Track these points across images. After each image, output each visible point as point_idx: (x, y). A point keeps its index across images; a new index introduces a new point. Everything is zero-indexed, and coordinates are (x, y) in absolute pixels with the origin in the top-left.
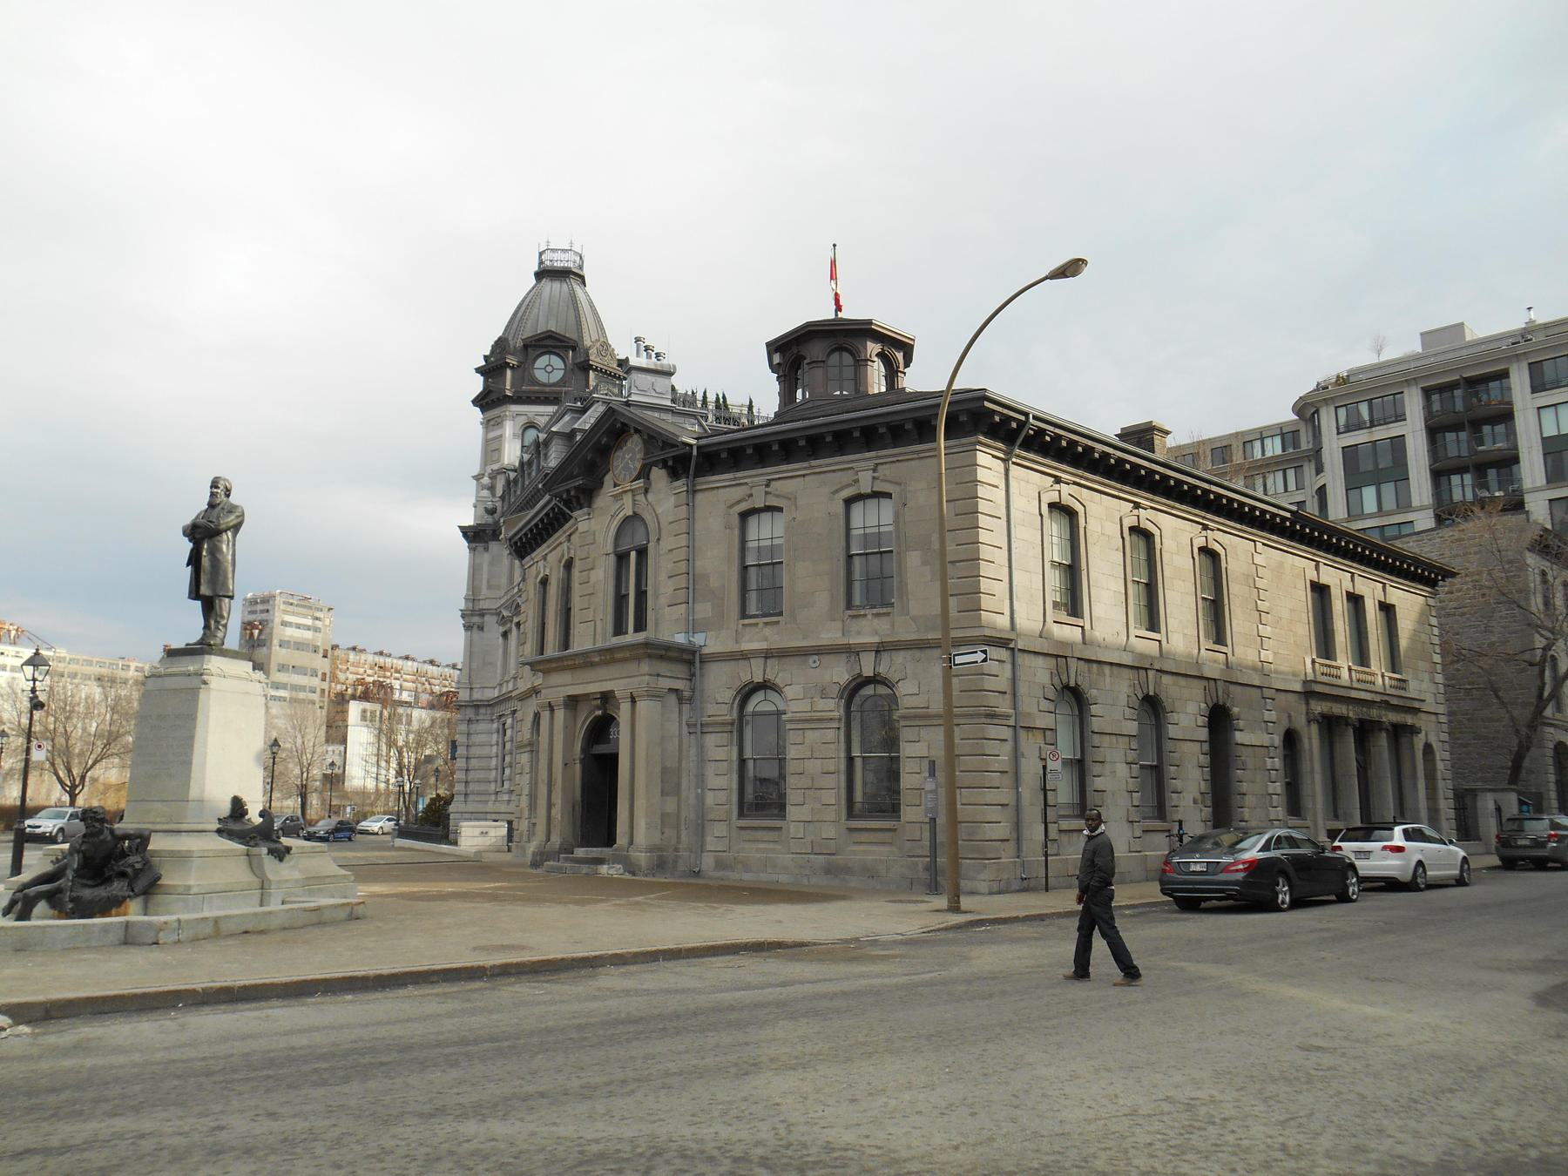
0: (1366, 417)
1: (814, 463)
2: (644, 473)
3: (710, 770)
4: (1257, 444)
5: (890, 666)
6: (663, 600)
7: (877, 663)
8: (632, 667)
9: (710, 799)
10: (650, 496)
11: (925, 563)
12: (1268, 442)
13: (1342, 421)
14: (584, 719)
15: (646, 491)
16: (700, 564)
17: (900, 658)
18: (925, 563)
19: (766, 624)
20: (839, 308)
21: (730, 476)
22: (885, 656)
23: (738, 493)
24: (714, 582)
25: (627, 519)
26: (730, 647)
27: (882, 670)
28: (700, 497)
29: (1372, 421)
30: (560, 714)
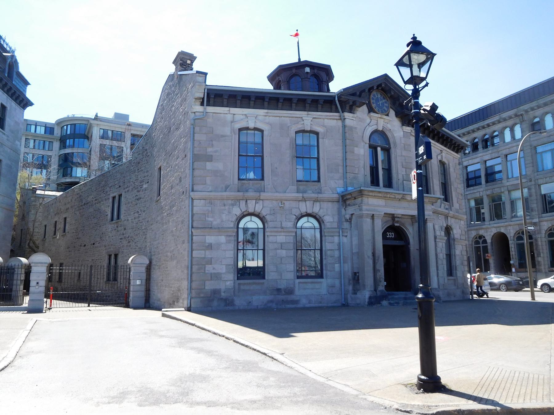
4: (33, 128)
12: (38, 128)
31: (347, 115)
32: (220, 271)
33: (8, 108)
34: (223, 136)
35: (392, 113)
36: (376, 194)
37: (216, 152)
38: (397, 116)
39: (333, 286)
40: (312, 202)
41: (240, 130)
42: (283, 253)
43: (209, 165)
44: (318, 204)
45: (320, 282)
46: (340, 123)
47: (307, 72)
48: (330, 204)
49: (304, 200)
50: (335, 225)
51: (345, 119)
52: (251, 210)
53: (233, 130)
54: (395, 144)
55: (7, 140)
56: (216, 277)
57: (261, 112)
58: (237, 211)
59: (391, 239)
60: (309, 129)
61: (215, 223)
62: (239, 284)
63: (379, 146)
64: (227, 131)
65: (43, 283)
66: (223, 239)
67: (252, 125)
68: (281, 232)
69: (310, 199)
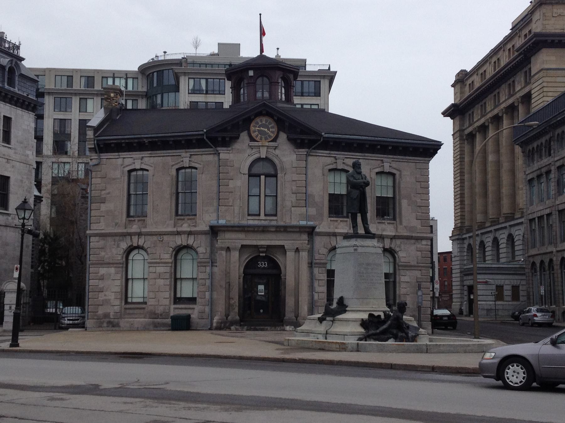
0: (204, 88)
1: (367, 155)
2: (274, 140)
3: (316, 284)
5: (395, 245)
6: (288, 204)
7: (391, 244)
8: (295, 236)
9: (316, 297)
10: (277, 151)
11: (409, 205)
13: (191, 87)
14: (246, 257)
15: (275, 149)
16: (310, 189)
17: (398, 242)
18: (409, 205)
19: (341, 221)
20: (262, 50)
21: (328, 152)
22: (394, 240)
23: (329, 160)
24: (317, 199)
25: (259, 159)
26: (328, 230)
27: (393, 246)
28: (310, 159)
29: (207, 91)
30: (235, 255)
31: (219, 149)
32: (110, 297)
33: (13, 119)
34: (114, 179)
35: (283, 136)
36: (230, 229)
37: (109, 193)
38: (289, 139)
39: (203, 312)
40: (186, 235)
41: (130, 172)
42: (161, 282)
43: (103, 207)
44: (193, 237)
45: (194, 309)
46: (216, 158)
47: (251, 76)
48: (204, 236)
49: (179, 233)
50: (207, 255)
51: (219, 153)
52: (135, 244)
53: (123, 173)
54: (283, 169)
55: (15, 153)
56: (106, 302)
57: (146, 154)
58: (124, 245)
59: (264, 268)
60: (188, 166)
61: (106, 256)
62: (126, 309)
63: (263, 175)
64: (118, 174)
65: (14, 307)
66: (112, 270)
67: (138, 167)
68: (159, 263)
69: (184, 233)
